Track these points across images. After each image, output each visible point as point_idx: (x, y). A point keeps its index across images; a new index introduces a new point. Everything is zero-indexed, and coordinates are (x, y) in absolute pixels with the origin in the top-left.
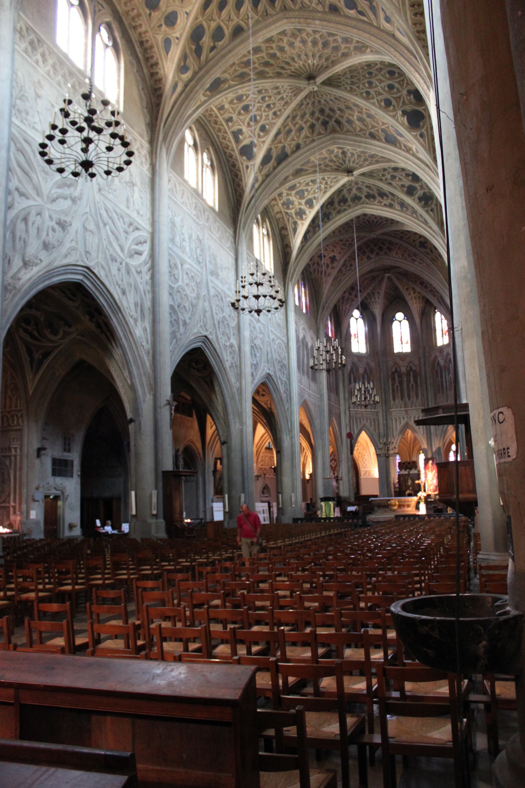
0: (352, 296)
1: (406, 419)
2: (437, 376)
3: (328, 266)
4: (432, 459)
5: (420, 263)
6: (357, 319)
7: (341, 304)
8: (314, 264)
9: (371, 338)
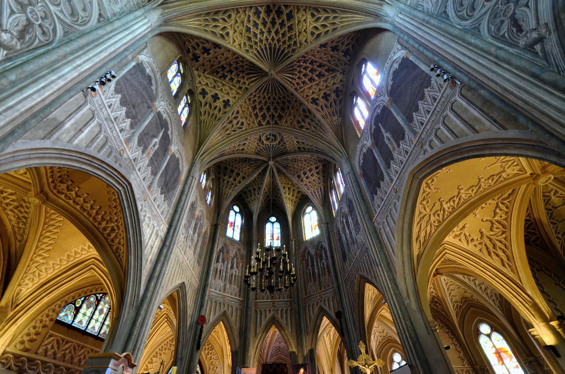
0: (236, 182)
1: (272, 312)
2: (308, 266)
3: (220, 110)
4: (304, 366)
5: (307, 129)
6: (236, 213)
7: (224, 188)
8: (206, 104)
9: (247, 229)
